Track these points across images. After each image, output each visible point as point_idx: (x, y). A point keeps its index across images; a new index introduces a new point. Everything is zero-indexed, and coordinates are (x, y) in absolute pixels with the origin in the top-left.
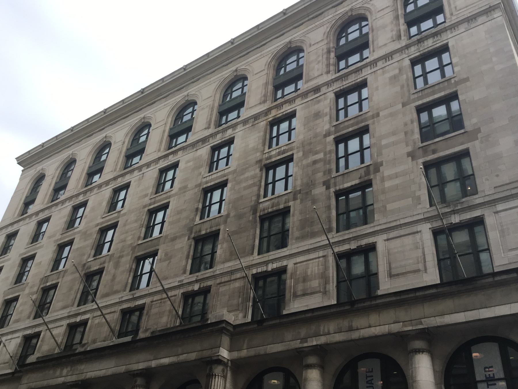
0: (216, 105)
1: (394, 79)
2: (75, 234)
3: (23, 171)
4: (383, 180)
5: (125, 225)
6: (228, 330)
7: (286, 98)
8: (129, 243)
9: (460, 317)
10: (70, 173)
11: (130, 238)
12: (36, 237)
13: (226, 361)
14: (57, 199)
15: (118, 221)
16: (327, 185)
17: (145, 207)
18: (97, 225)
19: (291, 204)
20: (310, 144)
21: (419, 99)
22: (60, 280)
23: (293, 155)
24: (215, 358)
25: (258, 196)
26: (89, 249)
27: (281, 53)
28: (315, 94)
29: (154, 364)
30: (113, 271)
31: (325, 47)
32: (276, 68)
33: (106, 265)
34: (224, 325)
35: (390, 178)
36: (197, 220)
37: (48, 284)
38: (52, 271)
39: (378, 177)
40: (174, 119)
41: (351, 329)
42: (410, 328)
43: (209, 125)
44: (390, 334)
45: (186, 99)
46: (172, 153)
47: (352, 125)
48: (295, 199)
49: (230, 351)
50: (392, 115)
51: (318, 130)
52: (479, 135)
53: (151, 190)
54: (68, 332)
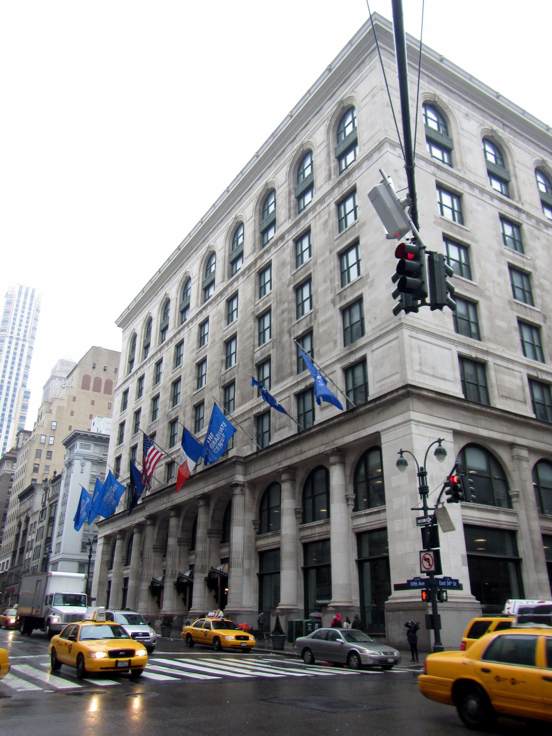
0: (227, 255)
1: (326, 223)
2: (159, 389)
3: (123, 332)
4: (318, 327)
5: (185, 379)
6: (240, 462)
7: (350, 168)
8: (189, 394)
9: (350, 438)
10: (189, 291)
11: (188, 390)
12: (178, 359)
13: (242, 483)
14: (209, 298)
15: (181, 376)
16: (290, 332)
17: (194, 361)
18: (170, 379)
19: (271, 352)
20: (280, 293)
21: (339, 244)
22: (156, 429)
23: (271, 305)
24: (234, 483)
25: (254, 346)
26: (168, 401)
27: (262, 196)
28: (282, 241)
29: (206, 490)
30: (183, 419)
31: (287, 189)
32: (261, 211)
33: (179, 414)
34: (234, 459)
35: (323, 324)
36: (224, 371)
37: (151, 432)
38: (153, 421)
39: (316, 324)
40: (205, 270)
41: (302, 453)
42: (328, 449)
43: (224, 277)
44: (320, 454)
45: (302, 150)
46: (210, 303)
47: (303, 273)
48: (273, 348)
49: (245, 475)
50: (323, 262)
51: (284, 280)
52: (369, 280)
53: (195, 346)
54: (167, 468)
